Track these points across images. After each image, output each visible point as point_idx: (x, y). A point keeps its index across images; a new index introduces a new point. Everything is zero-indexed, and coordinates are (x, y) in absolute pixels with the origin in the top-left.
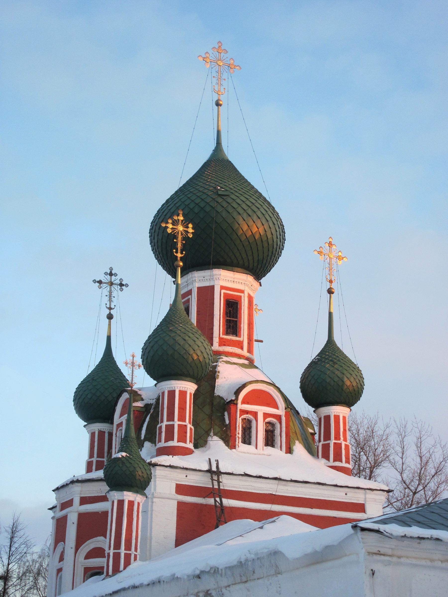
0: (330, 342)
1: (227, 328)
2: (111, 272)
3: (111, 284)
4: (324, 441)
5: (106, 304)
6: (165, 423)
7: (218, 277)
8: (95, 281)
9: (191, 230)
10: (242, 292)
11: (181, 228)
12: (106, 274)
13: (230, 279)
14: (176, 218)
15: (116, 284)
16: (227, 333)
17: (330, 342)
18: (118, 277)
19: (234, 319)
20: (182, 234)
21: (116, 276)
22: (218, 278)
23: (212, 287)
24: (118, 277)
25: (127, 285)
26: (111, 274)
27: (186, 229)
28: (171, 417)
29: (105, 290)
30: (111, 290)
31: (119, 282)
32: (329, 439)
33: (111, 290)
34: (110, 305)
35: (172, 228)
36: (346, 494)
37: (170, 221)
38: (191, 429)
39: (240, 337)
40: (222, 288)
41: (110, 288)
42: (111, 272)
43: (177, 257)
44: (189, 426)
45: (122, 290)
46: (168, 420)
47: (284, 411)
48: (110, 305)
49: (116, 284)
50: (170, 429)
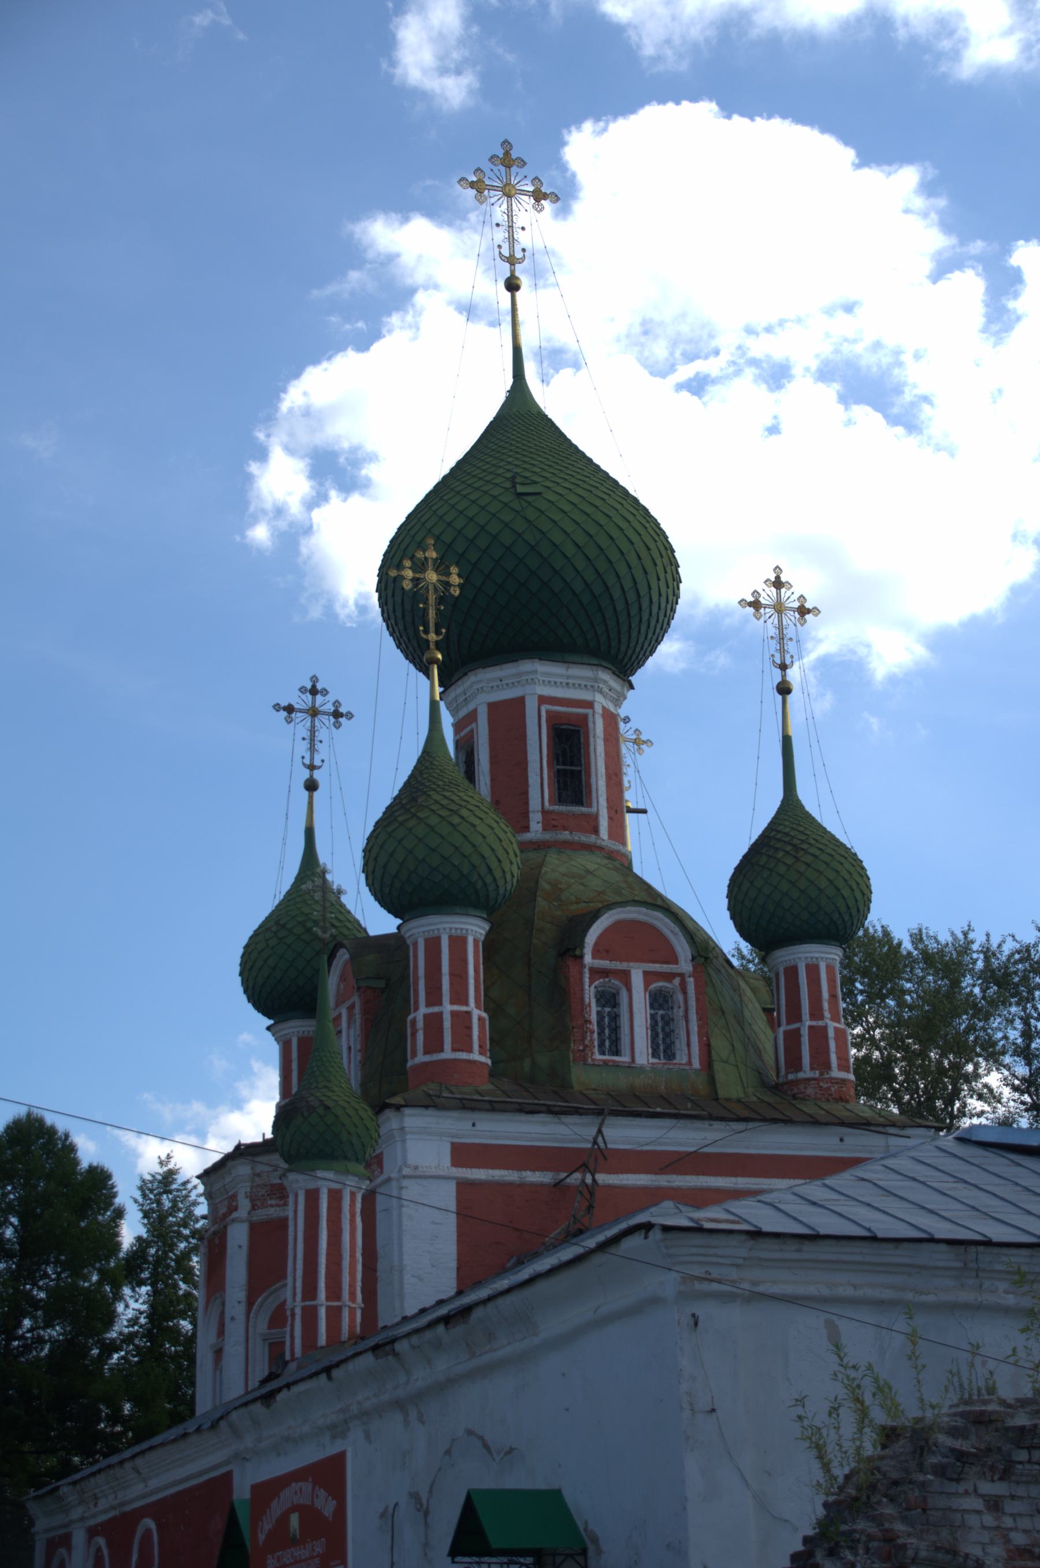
0: (790, 804)
1: (559, 788)
2: (314, 686)
4: (788, 1023)
5: (303, 757)
6: (423, 1010)
7: (532, 677)
8: (277, 707)
9: (455, 579)
10: (590, 705)
11: (432, 576)
12: (303, 690)
13: (558, 680)
14: (420, 555)
15: (325, 713)
16: (561, 801)
17: (790, 804)
18: (331, 698)
19: (573, 768)
20: (436, 590)
21: (324, 695)
22: (532, 679)
23: (520, 702)
24: (331, 698)
25: (349, 716)
26: (314, 691)
27: (444, 578)
28: (434, 997)
29: (302, 725)
30: (313, 726)
31: (332, 709)
32: (799, 1019)
33: (313, 726)
34: (312, 758)
35: (414, 580)
36: (841, 1140)
37: (407, 563)
38: (480, 1019)
39: (590, 806)
40: (543, 700)
42: (314, 686)
43: (427, 641)
44: (477, 1013)
45: (337, 725)
46: (428, 1005)
47: (691, 965)
48: (312, 758)
49: (325, 713)
50: (434, 1022)
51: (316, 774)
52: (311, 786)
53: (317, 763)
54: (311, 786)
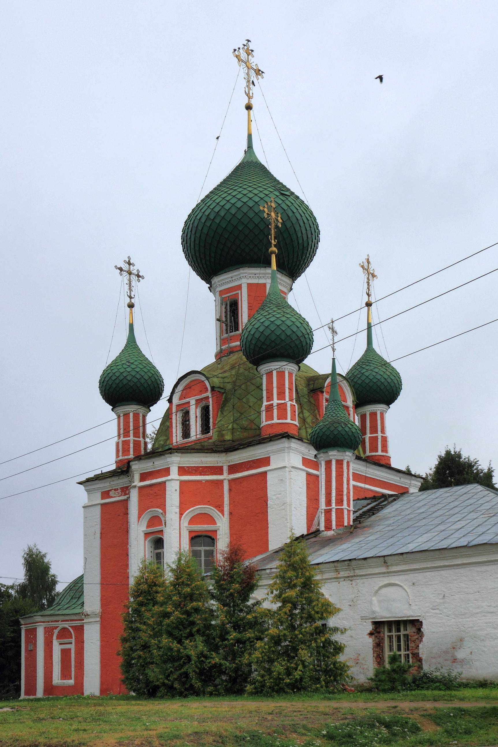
2: (129, 261)
3: (130, 273)
15: (134, 274)
21: (133, 266)
25: (143, 277)
34: (130, 294)
41: (130, 277)
42: (129, 261)
50: (269, 408)
51: (133, 300)
52: (131, 306)
53: (132, 296)
54: (131, 306)
